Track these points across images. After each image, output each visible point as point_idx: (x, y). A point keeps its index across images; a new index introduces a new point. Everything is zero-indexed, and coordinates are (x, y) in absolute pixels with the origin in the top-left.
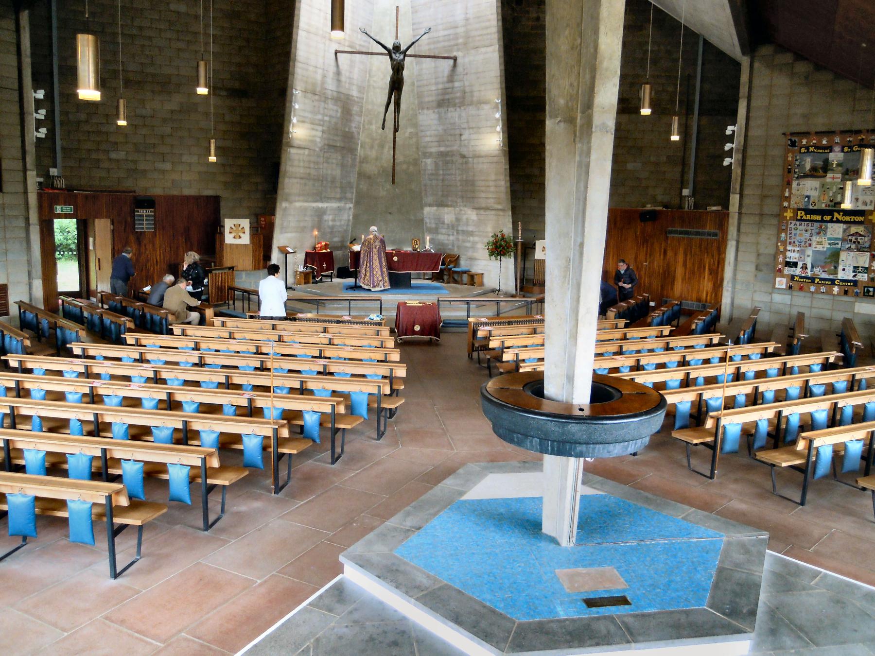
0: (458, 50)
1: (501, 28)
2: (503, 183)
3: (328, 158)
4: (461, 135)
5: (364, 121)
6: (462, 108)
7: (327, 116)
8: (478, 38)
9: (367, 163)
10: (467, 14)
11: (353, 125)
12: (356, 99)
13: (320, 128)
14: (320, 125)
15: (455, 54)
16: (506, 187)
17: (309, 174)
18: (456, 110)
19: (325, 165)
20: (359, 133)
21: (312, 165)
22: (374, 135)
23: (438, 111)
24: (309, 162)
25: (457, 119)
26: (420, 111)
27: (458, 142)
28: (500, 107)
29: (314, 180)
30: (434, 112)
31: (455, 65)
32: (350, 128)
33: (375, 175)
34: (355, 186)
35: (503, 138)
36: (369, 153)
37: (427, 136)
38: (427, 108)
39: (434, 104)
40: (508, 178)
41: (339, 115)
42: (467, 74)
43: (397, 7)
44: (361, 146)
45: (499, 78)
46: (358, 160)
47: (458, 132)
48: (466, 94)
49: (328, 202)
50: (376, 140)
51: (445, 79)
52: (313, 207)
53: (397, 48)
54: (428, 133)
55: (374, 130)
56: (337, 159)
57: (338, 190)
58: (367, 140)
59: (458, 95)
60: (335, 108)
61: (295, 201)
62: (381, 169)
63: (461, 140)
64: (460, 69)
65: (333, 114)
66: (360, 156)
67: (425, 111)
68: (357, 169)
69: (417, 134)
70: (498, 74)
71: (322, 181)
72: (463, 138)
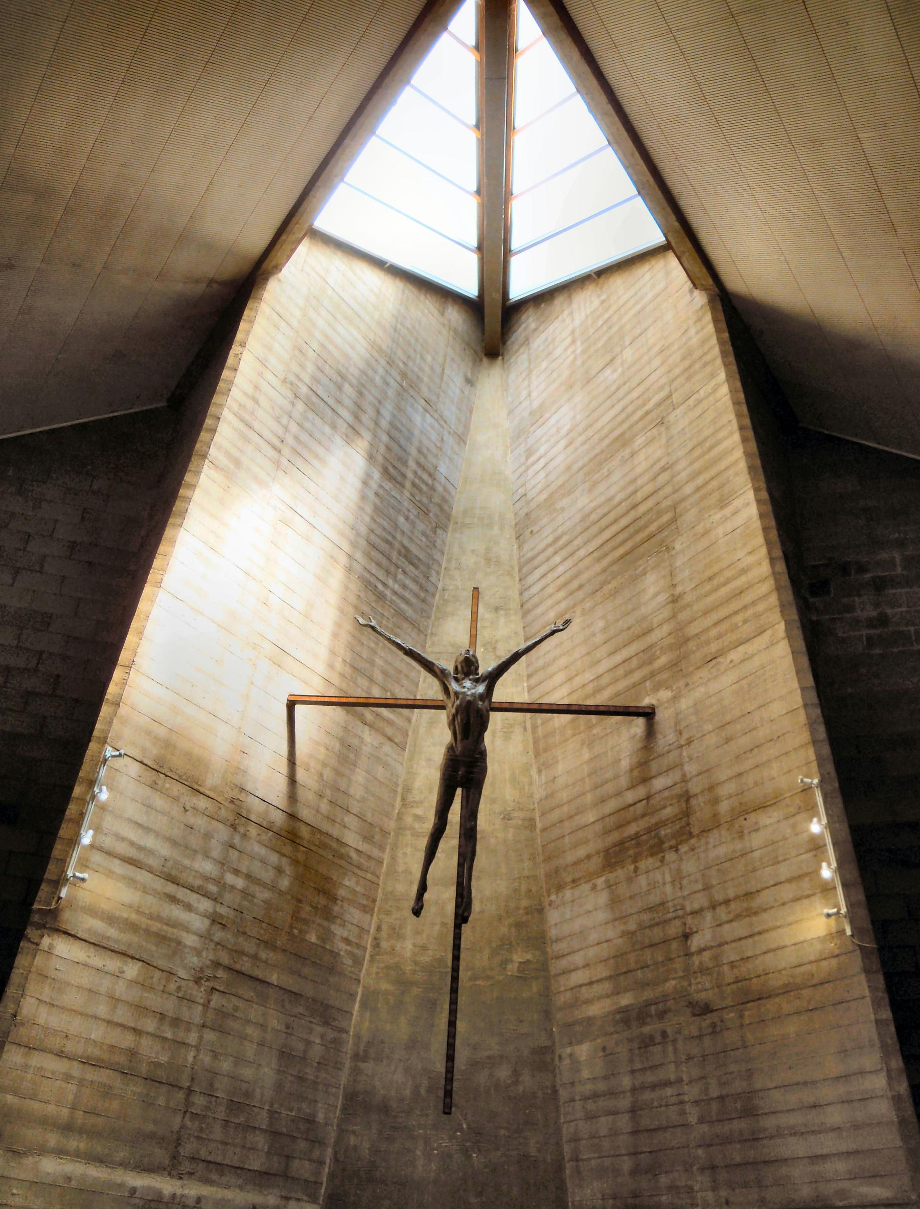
0: (656, 688)
1: (785, 580)
2: (879, 1082)
3: (221, 1013)
4: (686, 936)
5: (379, 929)
6: (684, 848)
7: (236, 872)
8: (713, 633)
9: (378, 1059)
10: (674, 586)
11: (338, 931)
12: (353, 855)
13: (205, 905)
14: (206, 895)
15: (646, 702)
16: (897, 1100)
17: (132, 1054)
18: (662, 860)
19: (209, 1036)
20: (358, 962)
21: (150, 1025)
22: (408, 968)
23: (607, 881)
24: (141, 1009)
25: (668, 888)
26: (553, 897)
27: (678, 965)
28: (819, 799)
29: (150, 1080)
30: (594, 888)
31: (651, 732)
32: (326, 936)
33: (402, 1100)
34: (332, 1134)
35: (850, 905)
36: (388, 1027)
37: (576, 969)
38: (574, 881)
39: (597, 862)
40: (897, 1062)
41: (285, 883)
42: (689, 742)
43: (476, 589)
44: (364, 1005)
45: (802, 713)
46: (349, 1047)
47: (674, 929)
48: (693, 802)
49: (207, 1181)
50: (413, 983)
51: (624, 782)
52: (133, 1190)
53: (468, 666)
54: (578, 959)
55: (408, 954)
56: (263, 1027)
57: (261, 1141)
58: (385, 986)
59: (668, 812)
60: (274, 858)
61: (42, 1150)
62: (425, 1083)
63: (688, 955)
64: (666, 737)
65: (267, 875)
66: (358, 1037)
67: (568, 894)
68: (344, 1077)
69: (544, 967)
70: (797, 699)
71: (190, 1091)
72: (696, 942)
